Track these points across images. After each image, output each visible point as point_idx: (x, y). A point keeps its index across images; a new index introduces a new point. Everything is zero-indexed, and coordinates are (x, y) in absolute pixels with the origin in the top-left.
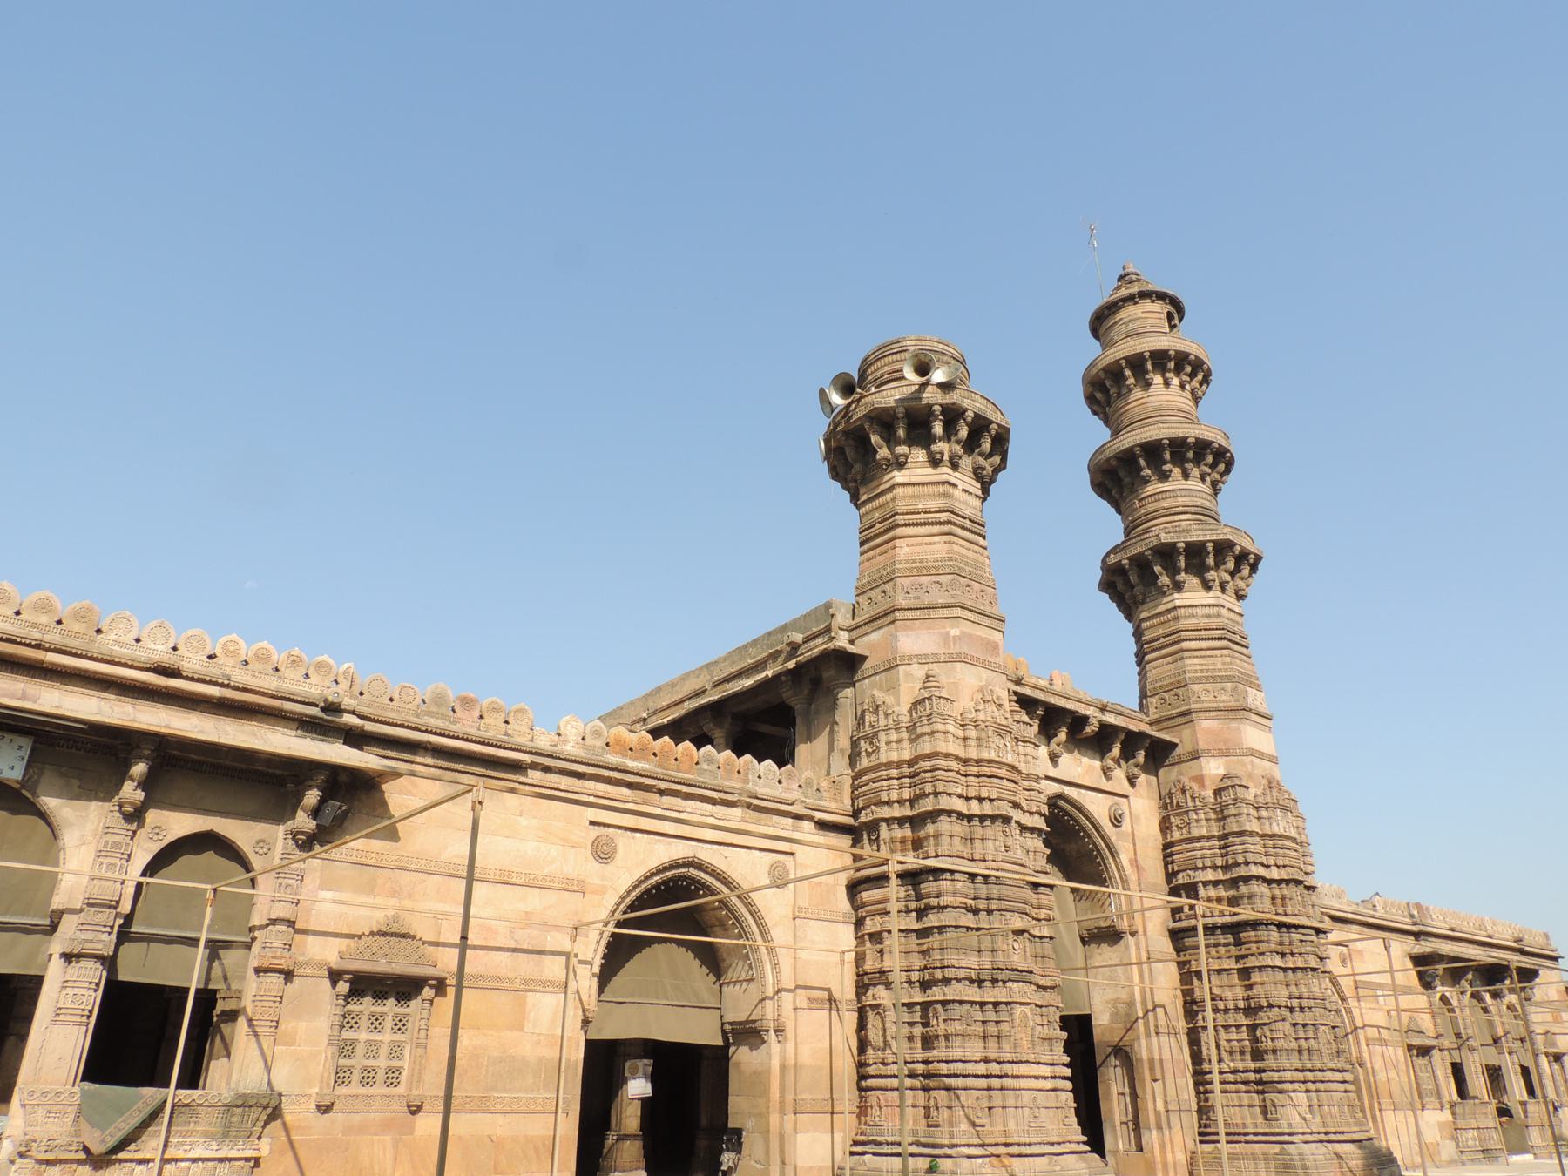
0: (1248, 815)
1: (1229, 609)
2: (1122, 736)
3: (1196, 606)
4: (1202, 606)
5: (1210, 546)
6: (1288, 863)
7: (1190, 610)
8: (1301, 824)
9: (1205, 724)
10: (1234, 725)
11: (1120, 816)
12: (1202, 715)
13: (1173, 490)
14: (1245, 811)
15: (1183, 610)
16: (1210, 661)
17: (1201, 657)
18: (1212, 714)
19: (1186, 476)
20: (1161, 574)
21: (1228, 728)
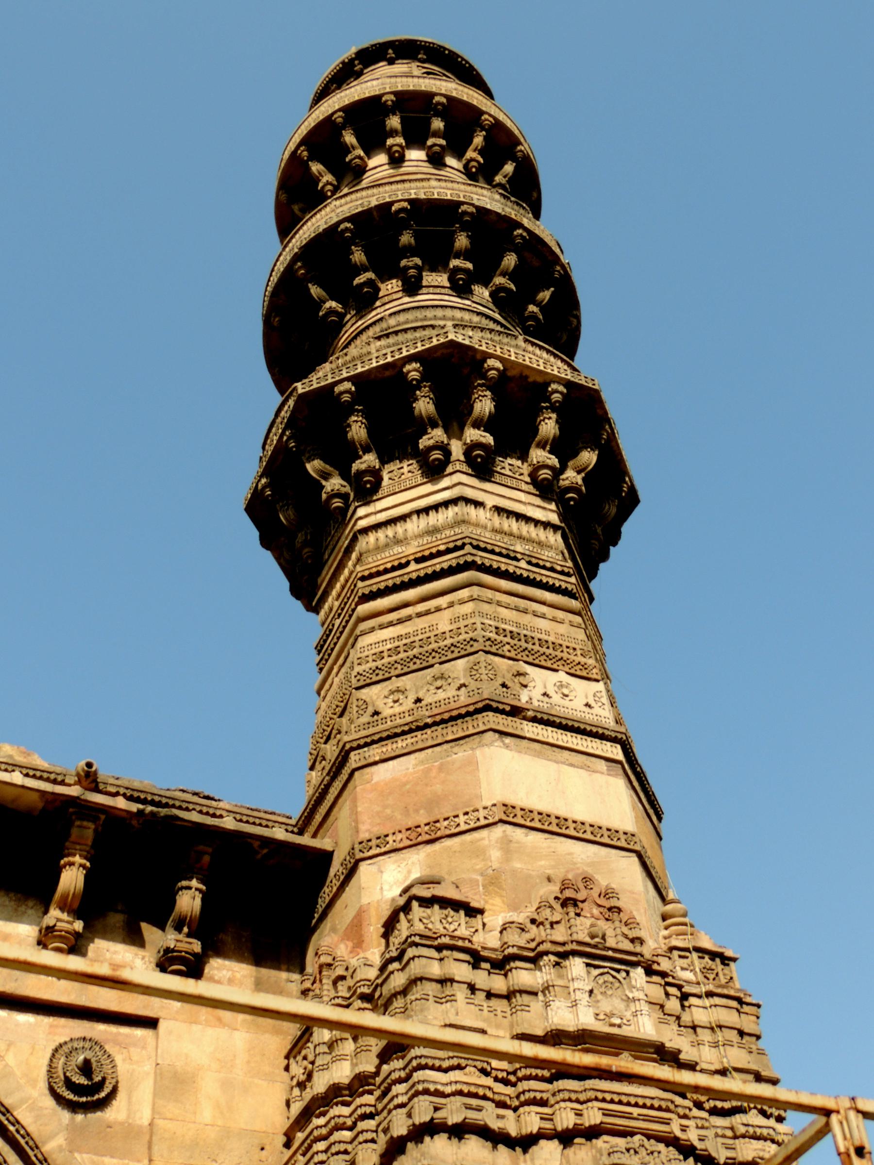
0: (445, 981)
1: (499, 510)
2: (87, 831)
3: (403, 518)
4: (419, 512)
5: (413, 371)
6: (593, 1116)
7: (390, 531)
8: (748, 1024)
9: (382, 773)
10: (461, 753)
11: (86, 1068)
12: (375, 752)
13: (381, 319)
14: (435, 969)
15: (371, 538)
16: (421, 623)
17: (400, 621)
18: (401, 744)
19: (412, 287)
20: (326, 476)
21: (441, 769)
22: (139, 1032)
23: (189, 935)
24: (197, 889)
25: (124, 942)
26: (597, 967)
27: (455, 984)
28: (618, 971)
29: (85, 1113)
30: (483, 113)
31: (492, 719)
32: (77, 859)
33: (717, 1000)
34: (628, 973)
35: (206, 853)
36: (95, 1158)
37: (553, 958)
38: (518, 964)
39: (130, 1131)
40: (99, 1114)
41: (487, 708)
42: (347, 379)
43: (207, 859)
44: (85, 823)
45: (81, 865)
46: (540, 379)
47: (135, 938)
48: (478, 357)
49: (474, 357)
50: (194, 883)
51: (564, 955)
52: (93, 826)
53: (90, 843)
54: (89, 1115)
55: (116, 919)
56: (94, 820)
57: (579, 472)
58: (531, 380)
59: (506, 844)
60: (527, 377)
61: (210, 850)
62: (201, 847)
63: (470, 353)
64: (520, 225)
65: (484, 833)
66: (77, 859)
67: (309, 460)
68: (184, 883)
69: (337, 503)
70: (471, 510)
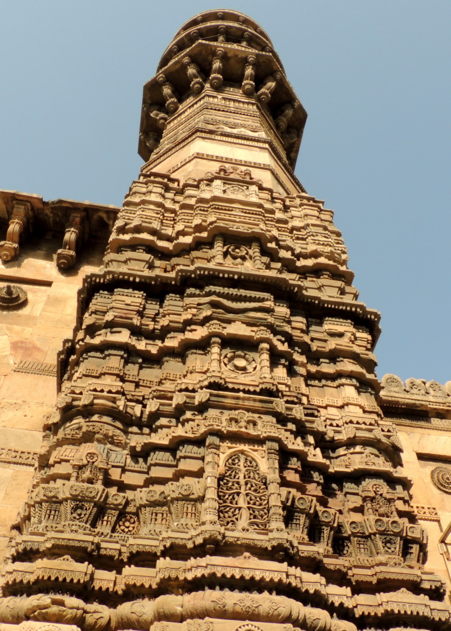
22: (43, 288)
23: (69, 249)
24: (73, 231)
25: (43, 259)
26: (229, 184)
27: (152, 194)
28: (243, 186)
29: (8, 312)
30: (239, 16)
31: (198, 134)
32: (16, 220)
33: (305, 207)
34: (248, 188)
35: (77, 217)
36: (9, 326)
37: (205, 182)
38: (189, 188)
39: (31, 320)
40: (15, 312)
41: (197, 131)
42: (161, 73)
43: (78, 219)
44: (20, 206)
45: (17, 223)
46: (244, 55)
47: (48, 257)
48: (213, 49)
49: (211, 49)
50: (72, 229)
51: (211, 181)
52: (23, 207)
53: (23, 215)
54: (10, 312)
55: (42, 252)
56: (25, 205)
57: (268, 90)
58: (240, 56)
59: (196, 165)
60: (237, 55)
61: (79, 215)
62: (75, 215)
63: (209, 48)
64: (247, 31)
65: (188, 165)
66: (16, 220)
67: (152, 112)
68: (67, 230)
69: (162, 121)
70: (211, 99)
